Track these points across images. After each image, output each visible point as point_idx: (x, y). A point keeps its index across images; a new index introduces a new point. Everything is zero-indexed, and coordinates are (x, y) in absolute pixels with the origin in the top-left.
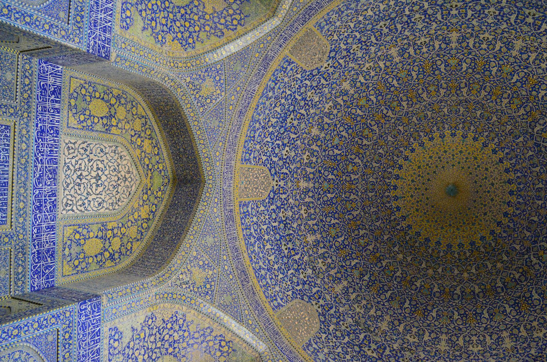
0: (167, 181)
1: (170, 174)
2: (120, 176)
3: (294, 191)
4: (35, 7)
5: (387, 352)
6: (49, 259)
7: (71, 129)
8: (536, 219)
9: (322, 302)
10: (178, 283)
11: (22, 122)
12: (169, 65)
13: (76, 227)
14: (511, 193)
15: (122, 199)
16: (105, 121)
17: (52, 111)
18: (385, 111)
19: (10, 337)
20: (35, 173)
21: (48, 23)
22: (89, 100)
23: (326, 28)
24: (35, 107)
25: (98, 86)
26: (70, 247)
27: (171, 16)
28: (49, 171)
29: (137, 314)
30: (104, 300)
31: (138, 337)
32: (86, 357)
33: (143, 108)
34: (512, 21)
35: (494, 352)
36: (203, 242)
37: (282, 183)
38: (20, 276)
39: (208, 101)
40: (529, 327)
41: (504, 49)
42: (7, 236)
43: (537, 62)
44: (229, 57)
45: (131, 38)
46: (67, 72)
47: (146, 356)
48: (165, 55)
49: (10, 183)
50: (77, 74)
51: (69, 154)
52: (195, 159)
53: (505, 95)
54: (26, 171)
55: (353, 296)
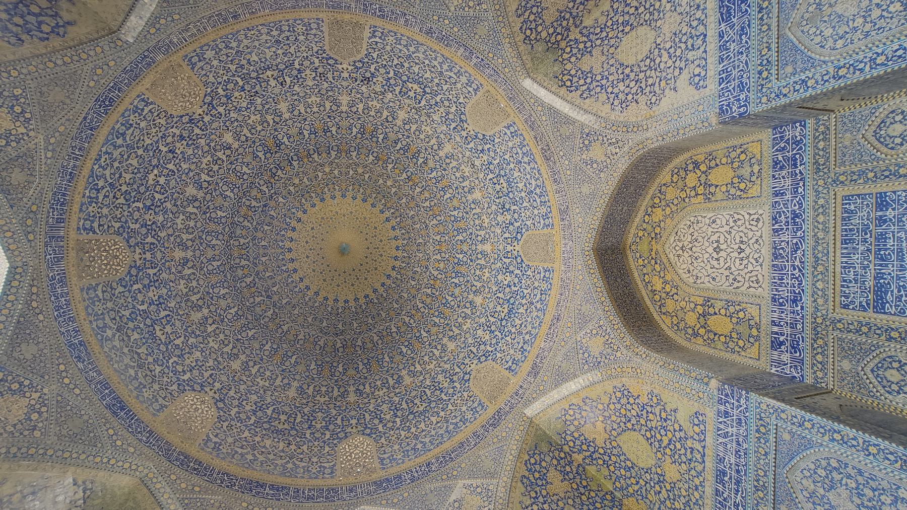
0: (633, 247)
1: (630, 255)
3: (496, 240)
4: (827, 449)
5: (398, 89)
6: (780, 158)
8: (266, 228)
9: (464, 134)
10: (620, 144)
11: (824, 312)
13: (745, 196)
14: (290, 250)
16: (711, 310)
17: (782, 323)
18: (412, 321)
19: (852, 65)
20: (803, 255)
21: (807, 428)
22: (733, 334)
23: (476, 405)
24: (806, 328)
26: (752, 174)
29: (671, 106)
30: (714, 120)
32: (738, 52)
33: (665, 324)
34: (299, 415)
35: (296, 97)
36: (593, 187)
37: (509, 248)
38: (821, 137)
39: (594, 332)
40: (265, 125)
41: (305, 387)
42: (842, 182)
43: (274, 377)
44: (575, 376)
45: (691, 403)
46: (763, 364)
49: (838, 244)
50: (751, 362)
51: (757, 276)
53: (301, 342)
55: (433, 141)
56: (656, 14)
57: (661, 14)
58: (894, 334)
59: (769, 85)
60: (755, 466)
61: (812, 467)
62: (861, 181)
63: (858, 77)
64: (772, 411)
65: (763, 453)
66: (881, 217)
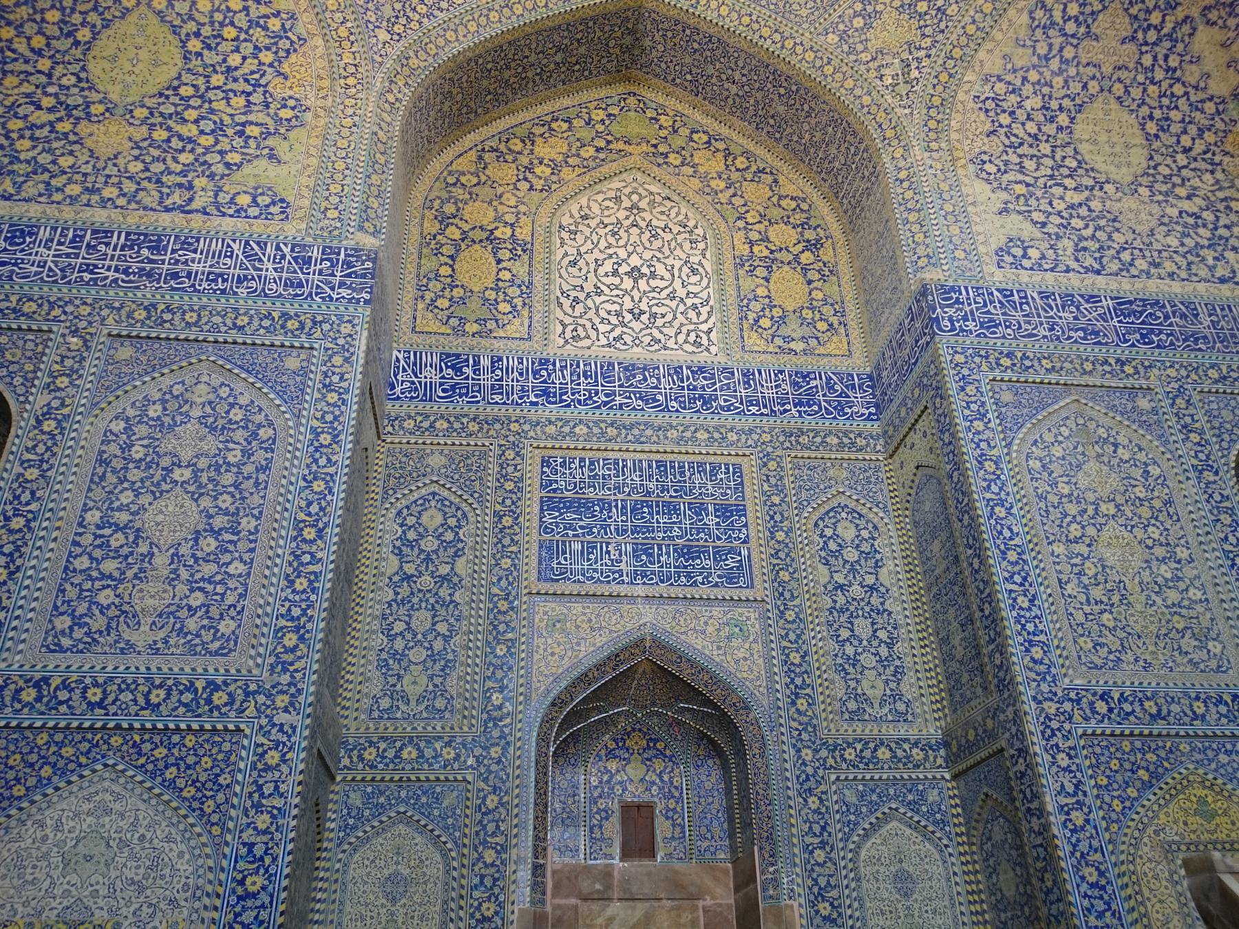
0: (632, 101)
2: (627, 223)
6: (813, 383)
7: (534, 332)
10: (903, 89)
11: (532, 434)
12: (354, 90)
15: (681, 217)
24: (496, 408)
25: (424, 270)
26: (788, 339)
27: (217, 80)
28: (628, 379)
29: (971, 199)
30: (932, 275)
31: (1022, 200)
33: (459, 154)
36: (804, 12)
38: (846, 440)
42: (765, 465)
45: (305, 192)
47: (1067, 182)
48: (330, 99)
49: (658, 457)
50: (406, 318)
52: (583, 21)
54: (632, 426)
56: (1164, 188)
57: (1161, 198)
58: (507, 521)
59: (984, 368)
60: (203, 307)
61: (243, 401)
62: (766, 487)
63: (976, 482)
64: (341, 341)
65: (239, 323)
66: (706, 509)
